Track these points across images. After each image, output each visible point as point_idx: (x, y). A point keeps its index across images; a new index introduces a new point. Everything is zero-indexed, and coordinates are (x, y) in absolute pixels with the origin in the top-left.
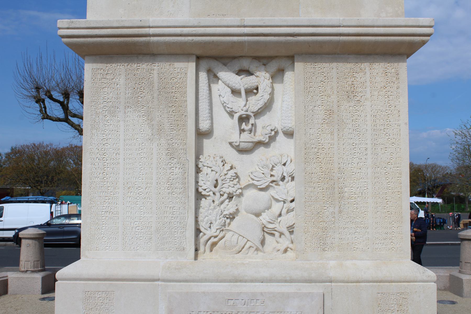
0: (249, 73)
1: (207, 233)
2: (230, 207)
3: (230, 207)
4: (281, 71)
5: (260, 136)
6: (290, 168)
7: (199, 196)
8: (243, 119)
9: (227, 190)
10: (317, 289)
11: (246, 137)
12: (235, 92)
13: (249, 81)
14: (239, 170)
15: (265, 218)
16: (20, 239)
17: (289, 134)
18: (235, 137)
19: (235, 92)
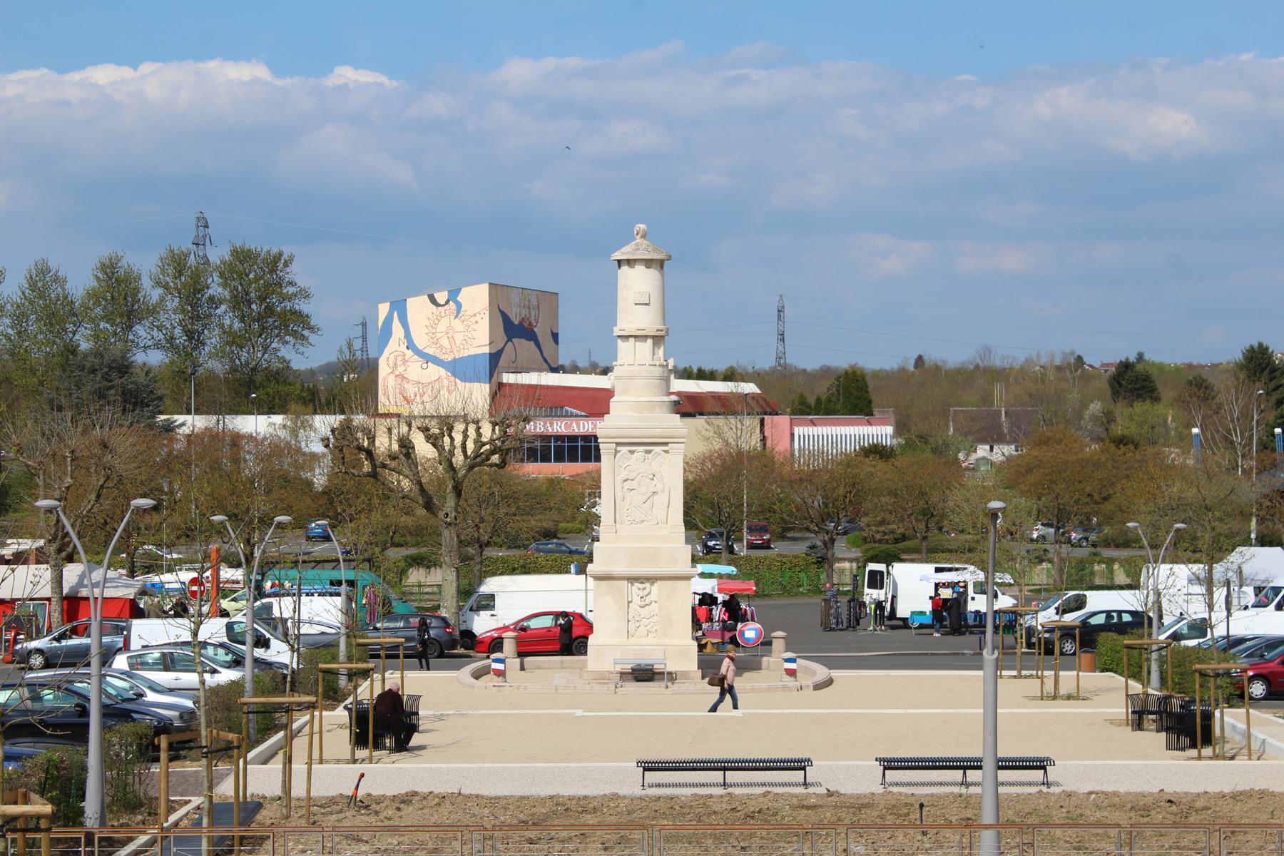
0: (643, 583)
1: (631, 632)
2: (638, 624)
3: (638, 624)
4: (653, 582)
5: (647, 602)
6: (656, 612)
7: (628, 621)
8: (642, 597)
9: (637, 618)
10: (663, 648)
11: (643, 603)
12: (639, 589)
13: (643, 586)
14: (641, 613)
15: (648, 627)
16: (503, 638)
17: (656, 602)
18: (639, 603)
19: (639, 589)
